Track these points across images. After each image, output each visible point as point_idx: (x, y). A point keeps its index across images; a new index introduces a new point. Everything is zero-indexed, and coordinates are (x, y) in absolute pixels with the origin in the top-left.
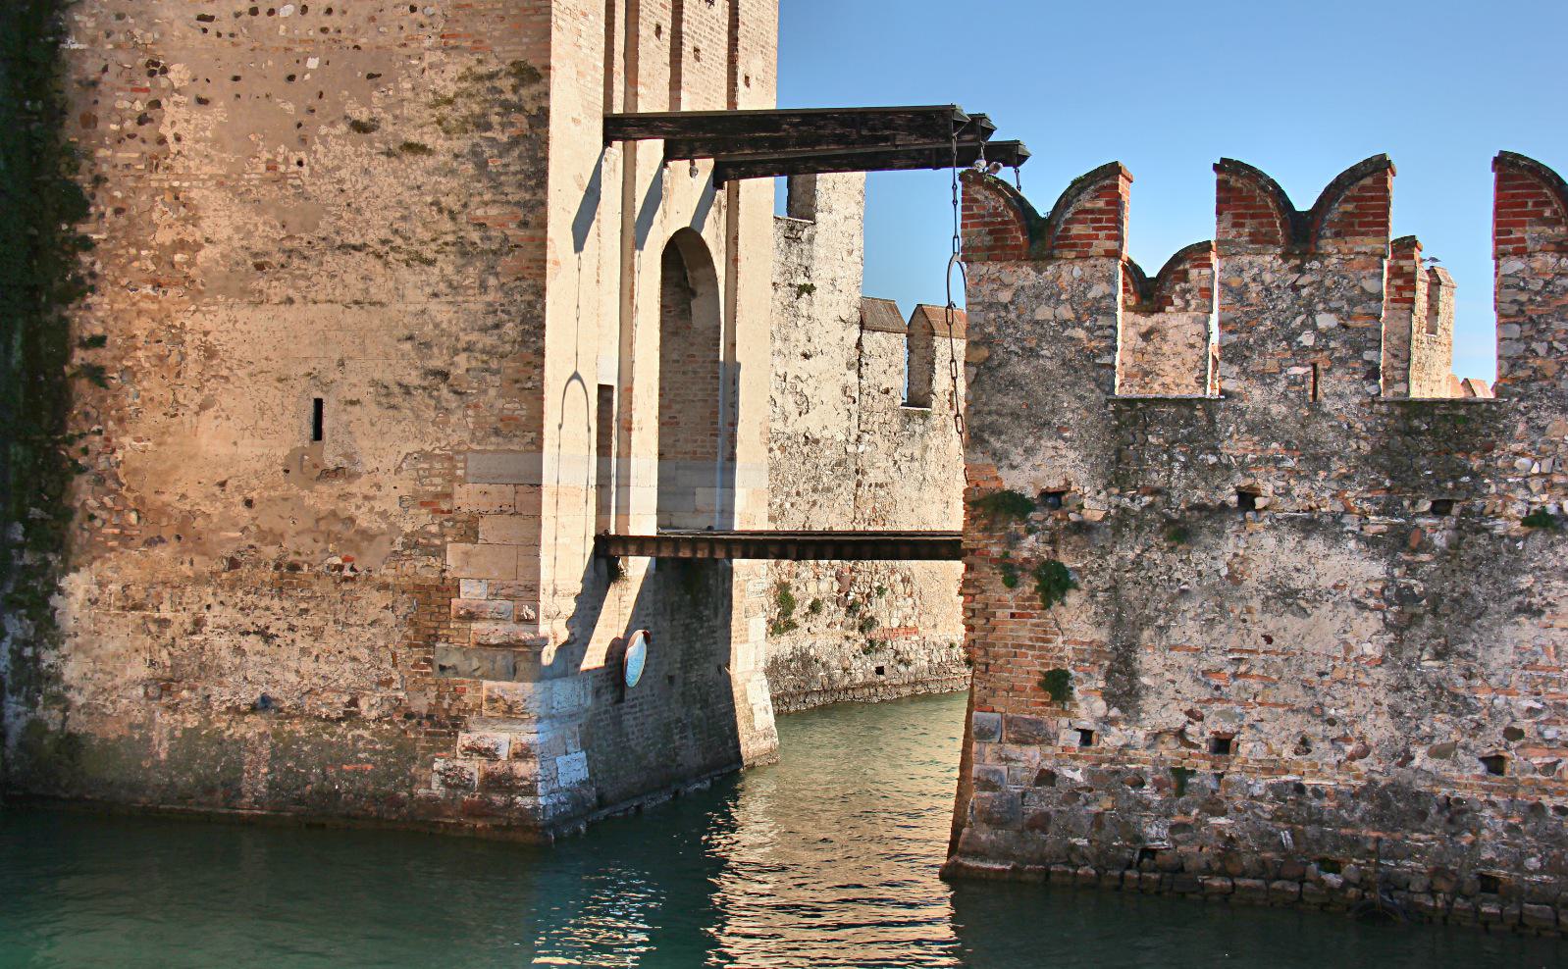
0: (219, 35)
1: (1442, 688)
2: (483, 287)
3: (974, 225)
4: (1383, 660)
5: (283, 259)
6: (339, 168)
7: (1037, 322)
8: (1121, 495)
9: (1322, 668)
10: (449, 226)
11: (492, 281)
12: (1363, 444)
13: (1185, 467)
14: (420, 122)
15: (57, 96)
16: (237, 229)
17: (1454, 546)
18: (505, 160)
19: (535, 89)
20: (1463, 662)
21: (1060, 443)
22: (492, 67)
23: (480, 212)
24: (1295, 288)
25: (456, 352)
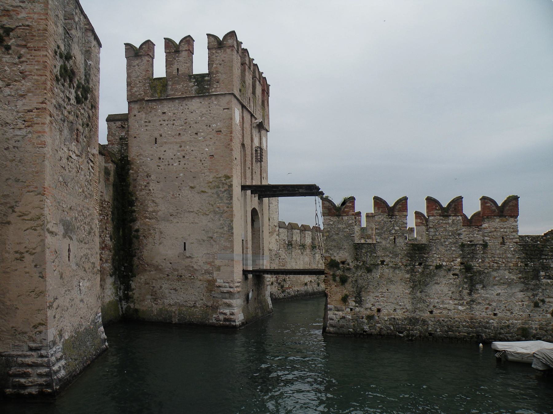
0: (161, 169)
1: (421, 299)
2: (220, 220)
3: (324, 208)
4: (410, 294)
5: (176, 214)
7: (338, 228)
8: (357, 262)
9: (398, 295)
10: (212, 207)
11: (221, 219)
12: (405, 252)
13: (370, 257)
14: (205, 186)
15: (128, 182)
16: (166, 208)
17: (423, 272)
18: (223, 194)
20: (425, 293)
21: (344, 252)
23: (218, 205)
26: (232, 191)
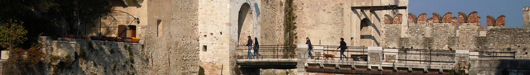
2: (337, 28)
6: (322, 15)
10: (333, 21)
11: (338, 27)
19: (342, 6)
22: (338, 4)
24: (416, 26)
25: (334, 34)
26: (343, 12)
